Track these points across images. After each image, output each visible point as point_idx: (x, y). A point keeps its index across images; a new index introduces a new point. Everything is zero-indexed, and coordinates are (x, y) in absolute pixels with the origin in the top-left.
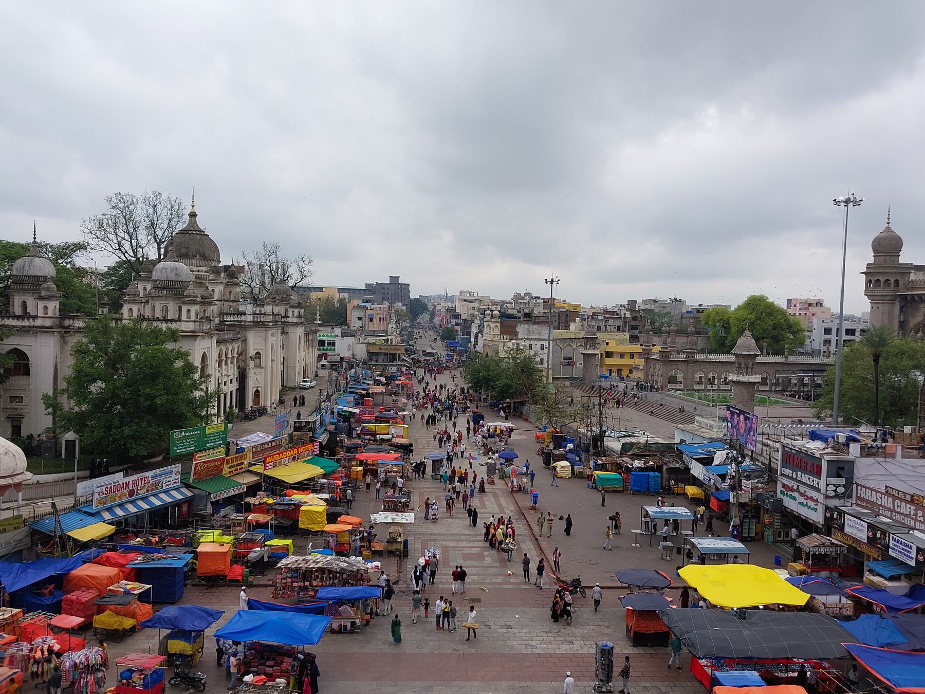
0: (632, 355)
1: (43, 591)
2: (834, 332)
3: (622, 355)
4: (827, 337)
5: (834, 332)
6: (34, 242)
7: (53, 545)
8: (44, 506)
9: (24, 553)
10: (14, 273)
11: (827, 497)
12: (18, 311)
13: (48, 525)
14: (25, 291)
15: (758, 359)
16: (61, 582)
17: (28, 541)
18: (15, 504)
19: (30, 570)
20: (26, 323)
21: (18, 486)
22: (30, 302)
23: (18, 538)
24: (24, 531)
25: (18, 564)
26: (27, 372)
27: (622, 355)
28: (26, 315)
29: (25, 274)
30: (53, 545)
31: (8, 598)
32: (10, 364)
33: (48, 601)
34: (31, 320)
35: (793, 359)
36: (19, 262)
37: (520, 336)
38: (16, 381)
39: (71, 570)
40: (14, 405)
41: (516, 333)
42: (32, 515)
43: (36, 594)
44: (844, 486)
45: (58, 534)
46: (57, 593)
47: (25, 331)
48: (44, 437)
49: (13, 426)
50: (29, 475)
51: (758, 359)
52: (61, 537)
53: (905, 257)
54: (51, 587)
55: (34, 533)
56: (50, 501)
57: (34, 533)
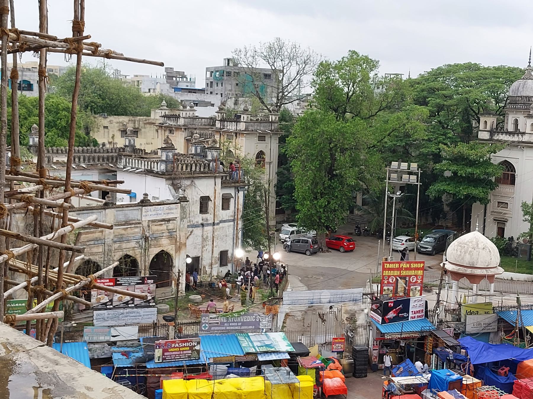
1: (500, 370)
6: (529, 66)
7: (514, 334)
8: (510, 300)
9: (492, 335)
10: (511, 94)
12: (511, 127)
13: (511, 317)
14: (517, 110)
16: (514, 366)
17: (495, 326)
18: (488, 293)
19: (491, 350)
20: (516, 138)
21: (491, 278)
22: (521, 119)
23: (487, 321)
24: (492, 317)
25: (482, 343)
26: (513, 182)
28: (517, 132)
29: (519, 95)
30: (514, 334)
31: (472, 368)
32: (500, 173)
33: (502, 380)
34: (520, 136)
36: (515, 84)
38: (504, 189)
39: (527, 358)
40: (499, 210)
42: (500, 305)
43: (493, 371)
45: (519, 325)
46: (511, 376)
47: (514, 146)
48: (521, 240)
49: (499, 228)
50: (501, 270)
52: (521, 330)
54: (507, 369)
55: (500, 320)
56: (514, 297)
57: (500, 320)
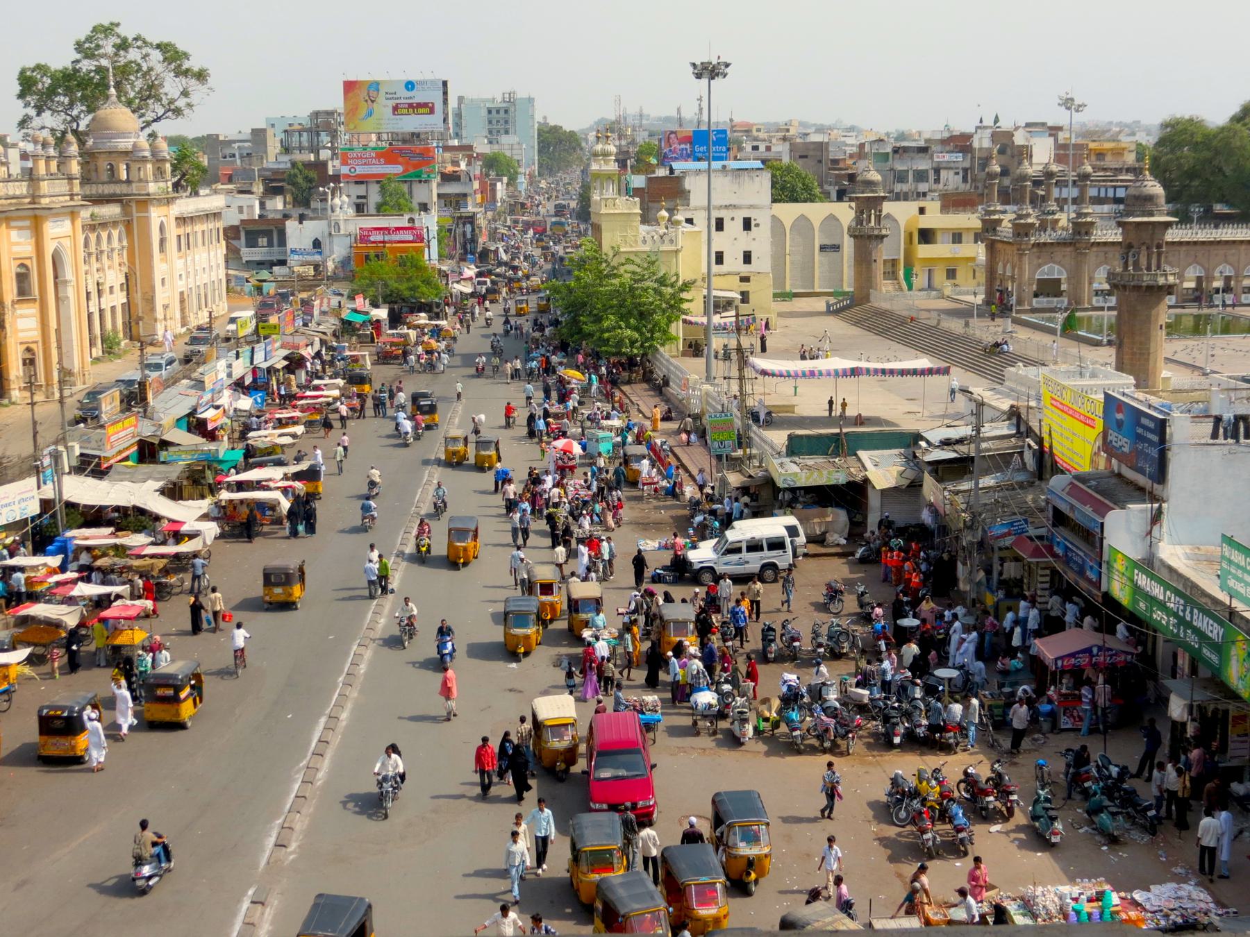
3: (957, 237)
15: (1172, 235)
27: (957, 237)
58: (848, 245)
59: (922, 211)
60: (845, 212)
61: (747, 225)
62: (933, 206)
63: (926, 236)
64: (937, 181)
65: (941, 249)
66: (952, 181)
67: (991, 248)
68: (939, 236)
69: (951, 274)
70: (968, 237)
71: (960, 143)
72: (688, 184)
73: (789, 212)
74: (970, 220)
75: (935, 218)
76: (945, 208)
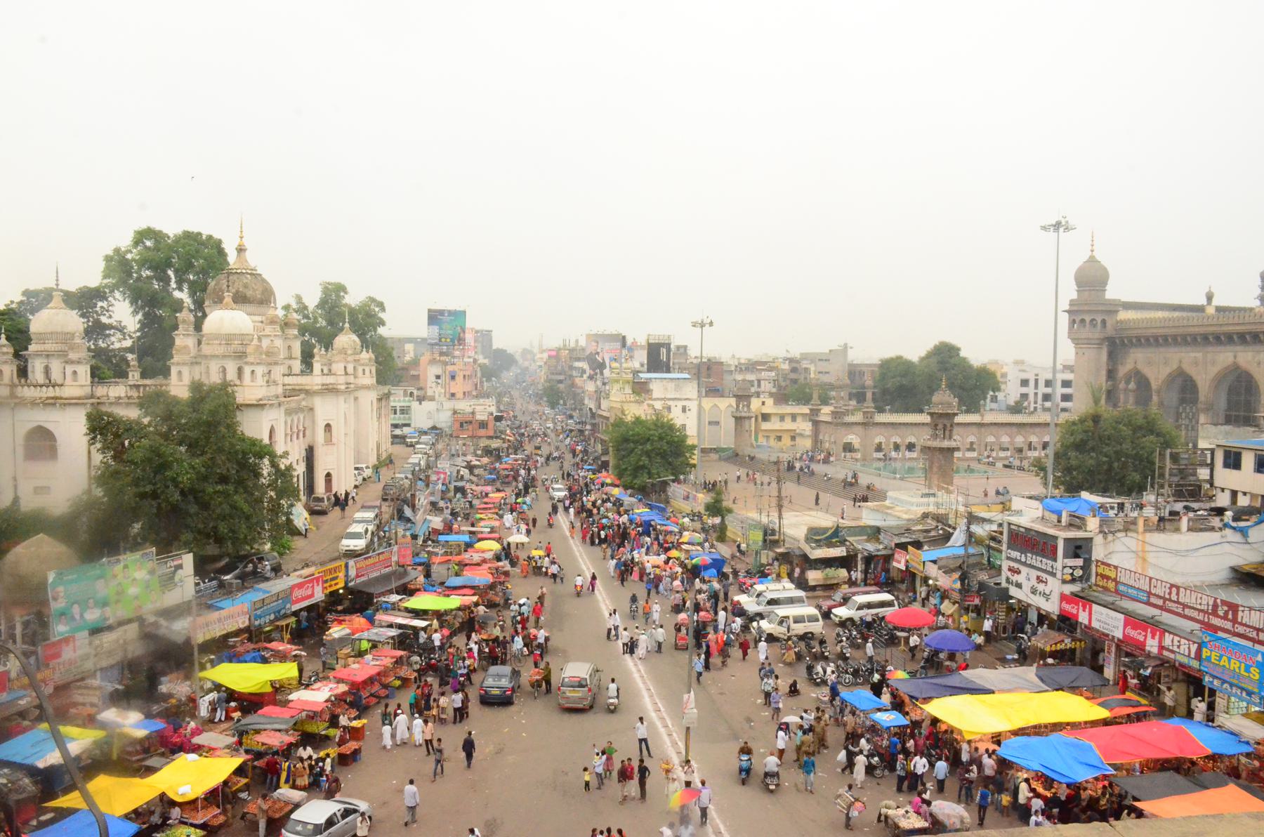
0: (794, 417)
2: (1032, 383)
3: (782, 418)
4: (1024, 390)
5: (1032, 383)
11: (1064, 582)
15: (960, 419)
35: (989, 418)
37: (655, 395)
41: (648, 391)
44: (1082, 568)
51: (958, 419)
53: (1113, 292)
58: (728, 424)
59: (763, 403)
60: (726, 405)
61: (684, 410)
62: (770, 402)
63: (766, 417)
64: (759, 386)
65: (774, 425)
66: (767, 386)
67: (816, 423)
68: (773, 419)
69: (779, 438)
70: (788, 419)
71: (768, 365)
72: (652, 386)
73: (708, 403)
74: (805, 410)
75: (770, 407)
76: (775, 404)
